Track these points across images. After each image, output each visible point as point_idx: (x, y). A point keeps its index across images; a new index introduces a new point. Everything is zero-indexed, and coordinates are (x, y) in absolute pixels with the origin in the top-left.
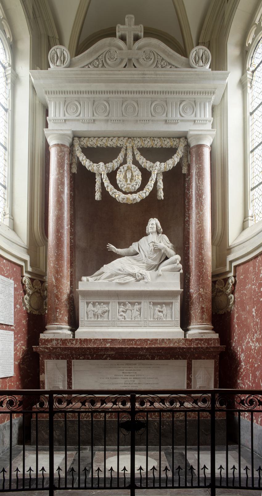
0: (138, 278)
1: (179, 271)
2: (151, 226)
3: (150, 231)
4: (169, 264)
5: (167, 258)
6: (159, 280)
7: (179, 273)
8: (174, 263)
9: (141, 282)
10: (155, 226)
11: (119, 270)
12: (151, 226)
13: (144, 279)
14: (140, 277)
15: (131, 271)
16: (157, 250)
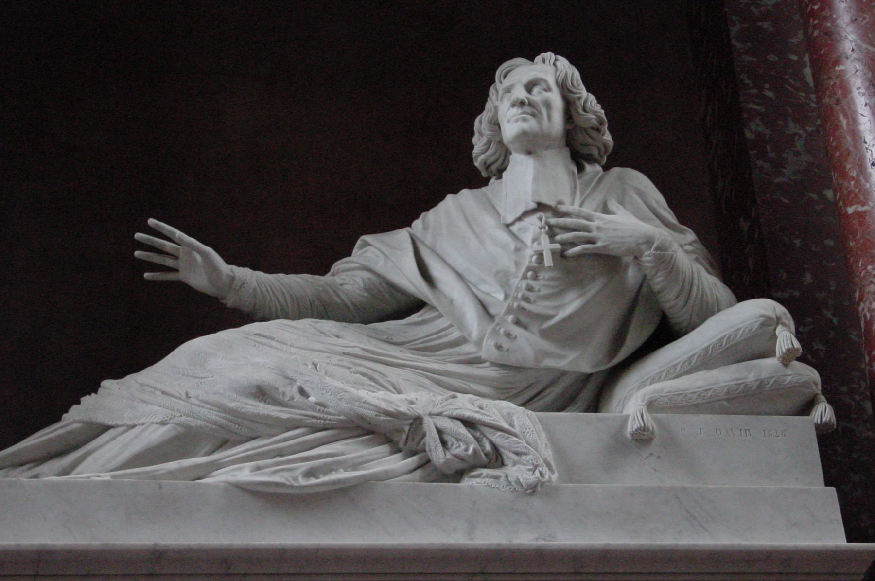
0: (438, 456)
1: (806, 408)
2: (520, 93)
3: (510, 130)
4: (707, 360)
5: (665, 333)
6: (639, 474)
7: (803, 430)
8: (752, 347)
9: (478, 482)
10: (557, 102)
11: (261, 393)
12: (520, 93)
13: (496, 459)
14: (465, 445)
15: (377, 399)
16: (581, 261)
